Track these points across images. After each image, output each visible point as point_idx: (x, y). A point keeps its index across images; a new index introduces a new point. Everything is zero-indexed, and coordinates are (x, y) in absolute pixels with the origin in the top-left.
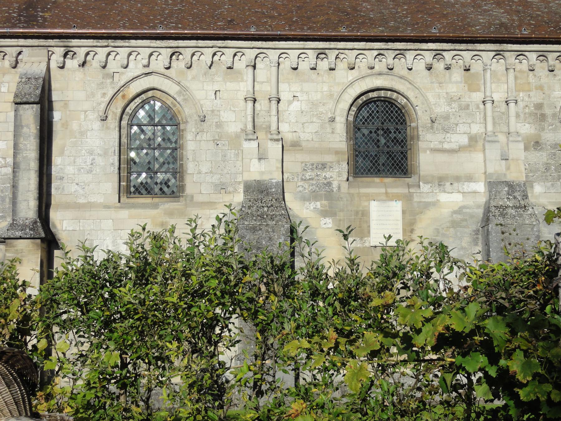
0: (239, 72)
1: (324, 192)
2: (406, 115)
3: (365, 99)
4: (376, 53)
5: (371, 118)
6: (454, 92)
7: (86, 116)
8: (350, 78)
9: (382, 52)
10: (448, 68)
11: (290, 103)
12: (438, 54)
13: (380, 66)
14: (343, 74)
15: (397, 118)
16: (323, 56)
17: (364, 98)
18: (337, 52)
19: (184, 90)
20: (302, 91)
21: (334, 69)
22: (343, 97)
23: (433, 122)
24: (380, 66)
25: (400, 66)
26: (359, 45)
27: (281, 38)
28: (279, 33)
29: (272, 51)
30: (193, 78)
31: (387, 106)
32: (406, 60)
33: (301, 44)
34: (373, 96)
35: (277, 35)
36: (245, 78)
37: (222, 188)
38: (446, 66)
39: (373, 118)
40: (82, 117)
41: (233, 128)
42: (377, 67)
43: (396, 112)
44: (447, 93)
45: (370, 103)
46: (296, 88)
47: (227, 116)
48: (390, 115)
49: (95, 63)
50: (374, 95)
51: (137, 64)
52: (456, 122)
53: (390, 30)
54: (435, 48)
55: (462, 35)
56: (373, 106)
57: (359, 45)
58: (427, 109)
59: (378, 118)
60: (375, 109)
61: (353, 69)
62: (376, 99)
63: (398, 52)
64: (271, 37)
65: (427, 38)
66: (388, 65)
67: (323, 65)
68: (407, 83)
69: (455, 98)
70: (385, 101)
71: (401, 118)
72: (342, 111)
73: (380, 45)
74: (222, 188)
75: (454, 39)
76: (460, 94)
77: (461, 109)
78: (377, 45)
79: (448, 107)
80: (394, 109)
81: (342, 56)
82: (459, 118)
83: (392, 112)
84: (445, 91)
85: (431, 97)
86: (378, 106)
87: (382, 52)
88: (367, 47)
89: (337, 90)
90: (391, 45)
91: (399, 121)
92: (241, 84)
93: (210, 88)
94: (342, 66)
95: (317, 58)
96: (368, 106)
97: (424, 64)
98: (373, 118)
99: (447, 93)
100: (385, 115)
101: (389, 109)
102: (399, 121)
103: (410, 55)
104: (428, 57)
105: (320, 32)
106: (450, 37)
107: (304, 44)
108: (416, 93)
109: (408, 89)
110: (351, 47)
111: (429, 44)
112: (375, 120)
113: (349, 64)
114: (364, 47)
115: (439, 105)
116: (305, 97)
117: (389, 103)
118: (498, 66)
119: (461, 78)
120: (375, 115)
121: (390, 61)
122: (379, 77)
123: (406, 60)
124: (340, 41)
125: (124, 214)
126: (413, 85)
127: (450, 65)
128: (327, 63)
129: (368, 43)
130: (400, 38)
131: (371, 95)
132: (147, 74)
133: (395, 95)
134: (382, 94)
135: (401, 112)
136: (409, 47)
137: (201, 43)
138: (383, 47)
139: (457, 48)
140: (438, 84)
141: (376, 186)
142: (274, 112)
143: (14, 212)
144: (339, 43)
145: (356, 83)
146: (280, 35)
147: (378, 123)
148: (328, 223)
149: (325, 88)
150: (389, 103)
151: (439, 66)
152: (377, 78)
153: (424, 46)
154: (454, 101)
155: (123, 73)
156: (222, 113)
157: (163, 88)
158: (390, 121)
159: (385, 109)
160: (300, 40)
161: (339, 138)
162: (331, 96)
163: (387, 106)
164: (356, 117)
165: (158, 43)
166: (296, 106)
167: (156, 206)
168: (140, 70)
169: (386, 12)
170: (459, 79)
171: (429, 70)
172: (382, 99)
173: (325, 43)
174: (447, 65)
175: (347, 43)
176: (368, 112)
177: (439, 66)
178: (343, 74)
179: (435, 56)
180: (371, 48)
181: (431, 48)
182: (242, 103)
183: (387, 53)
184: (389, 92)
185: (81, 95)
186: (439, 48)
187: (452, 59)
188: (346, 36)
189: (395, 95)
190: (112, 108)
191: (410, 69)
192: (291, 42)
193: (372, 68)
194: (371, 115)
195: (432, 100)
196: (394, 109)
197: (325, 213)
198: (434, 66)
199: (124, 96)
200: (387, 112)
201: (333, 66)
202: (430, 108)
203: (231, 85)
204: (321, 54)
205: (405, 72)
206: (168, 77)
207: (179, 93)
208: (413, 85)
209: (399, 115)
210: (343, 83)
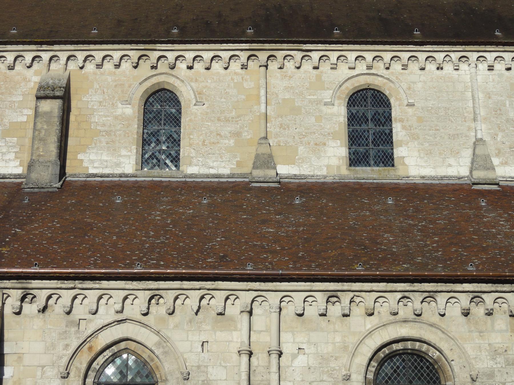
0: (232, 319)
2: (439, 371)
3: (387, 352)
4: (399, 295)
5: (395, 375)
6: (498, 343)
7: (43, 373)
8: (369, 326)
9: (406, 294)
10: (489, 314)
11: (294, 357)
12: (476, 297)
13: (405, 312)
14: (359, 322)
15: (428, 375)
16: (335, 299)
17: (386, 351)
18: (351, 294)
19: (164, 340)
20: (309, 342)
21: (349, 316)
22: (360, 350)
23: (473, 380)
24: (405, 312)
25: (430, 311)
26: (378, 286)
27: (283, 278)
28: (281, 272)
29: (272, 294)
30: (176, 326)
31: (415, 360)
32: (437, 303)
33: (308, 286)
34: (398, 348)
35: (278, 275)
36: (239, 326)
38: (487, 312)
39: (398, 375)
40: (39, 373)
42: (401, 313)
43: (428, 368)
44: (489, 344)
45: (395, 356)
46: (301, 338)
48: (419, 371)
49: (58, 308)
50: (399, 346)
52: (503, 380)
53: (416, 267)
54: (472, 289)
55: (504, 274)
56: (398, 360)
57: (378, 286)
58: (465, 364)
59: (404, 375)
60: (401, 364)
61: (372, 314)
62: (401, 352)
63: (427, 294)
64: (270, 277)
65: (462, 278)
66: (415, 310)
67: (335, 310)
68: (439, 333)
69: (500, 351)
70: (412, 354)
71: (434, 375)
73: (404, 287)
75: (495, 278)
76: (505, 345)
77: (508, 365)
78: (401, 286)
79: (491, 362)
80: (425, 364)
81: (357, 300)
82: (506, 375)
83: (422, 368)
84: (487, 342)
85: (470, 349)
86: (404, 360)
87: (406, 294)
88: (389, 289)
89: (352, 340)
90: (417, 286)
91: (431, 378)
92: (235, 334)
93: (198, 338)
94: (358, 311)
95: (327, 302)
96: (392, 361)
97: (460, 309)
98: (398, 375)
99: (489, 344)
100: (413, 371)
101: (419, 364)
102: (431, 378)
103: (442, 298)
104: (464, 300)
105: (331, 270)
106: (490, 276)
107: (310, 286)
108: (451, 344)
109: (441, 339)
110: (369, 289)
111: (465, 285)
112: (402, 378)
113: (367, 309)
114: (384, 289)
115: (480, 359)
116: (313, 350)
117: (419, 356)
119: (507, 326)
120: (401, 371)
121: (417, 305)
122: (404, 325)
123: (437, 303)
124: (355, 282)
126: (446, 334)
127: (492, 309)
128: (340, 308)
129: (389, 284)
130: (428, 278)
131: (395, 347)
132: (120, 322)
133: (425, 347)
134: (409, 345)
135: (434, 368)
136: (439, 289)
137: (186, 284)
138: (408, 288)
139: (499, 289)
140: (478, 334)
142: (274, 368)
144: (353, 284)
145: (376, 333)
146: (282, 275)
147: (404, 381)
149: (338, 339)
150: (418, 356)
151: (479, 311)
152: (401, 326)
153: (459, 287)
154: (500, 354)
155: (91, 321)
156: (210, 369)
157: (139, 339)
158: (419, 379)
159: (413, 364)
160: (305, 281)
162: (345, 348)
163: (415, 360)
164: (377, 374)
165: (135, 284)
166: (301, 361)
168: (113, 317)
169: (412, 245)
170: (504, 327)
171: (466, 316)
172: (409, 351)
173: (336, 284)
174: (488, 309)
175: (364, 284)
176: (392, 368)
177: (479, 311)
178: (359, 322)
179: (472, 299)
180: (393, 289)
181: (467, 289)
182: (235, 356)
183: (414, 296)
184: (418, 344)
185: (38, 347)
186: (477, 289)
187: (494, 303)
188: (363, 275)
189: (425, 347)
190: (76, 362)
191: (443, 315)
192: (296, 283)
193: (396, 314)
194: (395, 371)
195: (471, 353)
196: (425, 364)
198: (471, 311)
199: (90, 348)
200: (416, 368)
201: (347, 312)
202: (469, 364)
203: (221, 335)
204: (332, 297)
205: (436, 319)
206: (145, 326)
207: (158, 344)
208: (446, 334)
209: (431, 371)
210: (360, 332)
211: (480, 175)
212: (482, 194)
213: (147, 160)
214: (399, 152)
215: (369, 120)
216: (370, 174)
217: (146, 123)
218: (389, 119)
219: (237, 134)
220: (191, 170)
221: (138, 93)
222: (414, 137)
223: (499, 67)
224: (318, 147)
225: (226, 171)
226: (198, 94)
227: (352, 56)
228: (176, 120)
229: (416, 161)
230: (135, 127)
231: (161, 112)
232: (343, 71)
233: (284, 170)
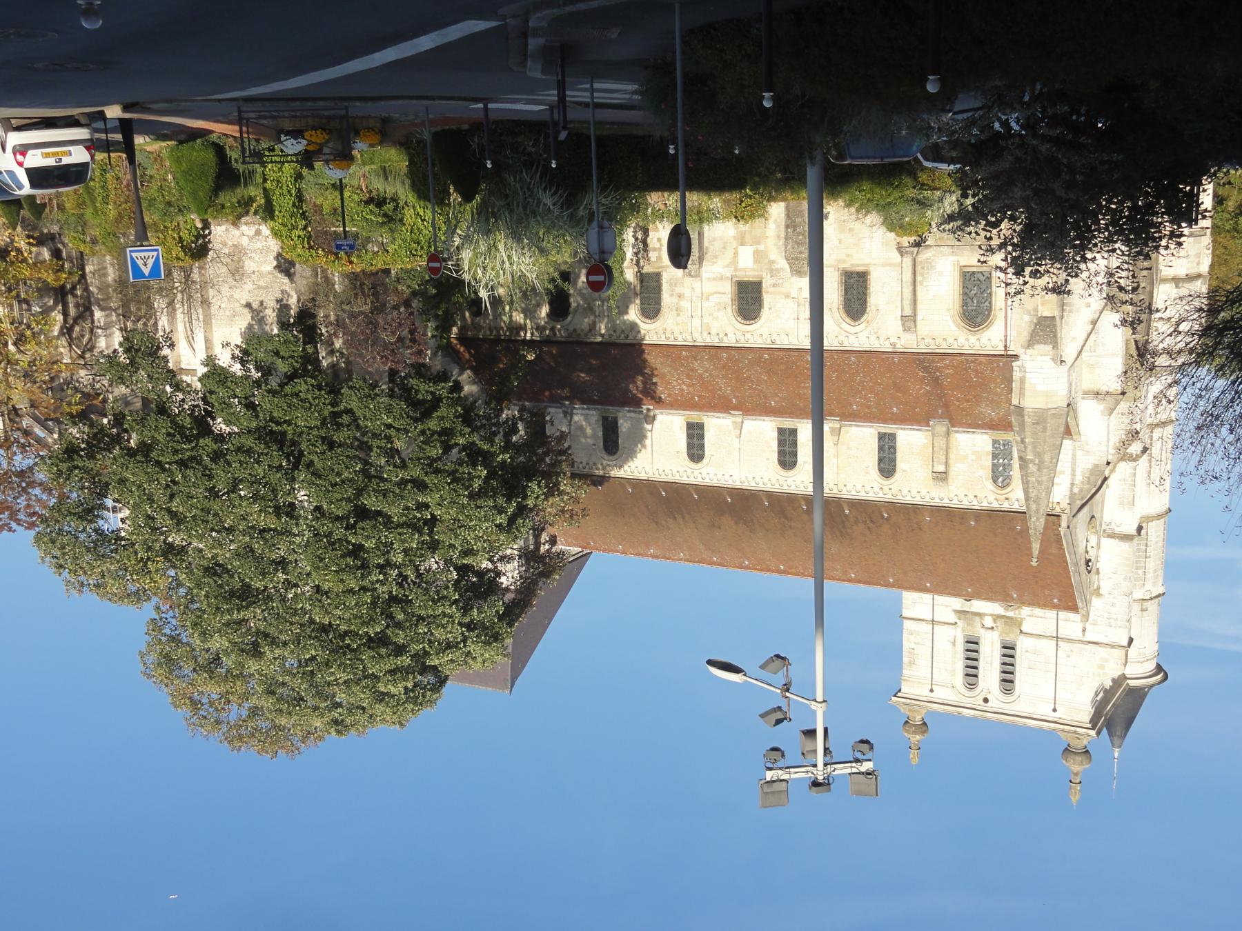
1: (773, 273)
12: (721, 341)
13: (748, 336)
72: (765, 312)
104: (725, 339)
118: (696, 335)
125: (866, 261)
141: (750, 276)
143: (914, 260)
148: (772, 258)
150: (745, 318)
161: (767, 299)
167: (852, 265)
177: (721, 335)
197: (773, 262)
213: (893, 437)
214: (776, 434)
216: (788, 423)
217: (895, 460)
218: (779, 453)
220: (872, 430)
221: (897, 475)
223: (727, 477)
225: (854, 428)
227: (793, 487)
228: (880, 460)
230: (899, 456)
231: (887, 465)
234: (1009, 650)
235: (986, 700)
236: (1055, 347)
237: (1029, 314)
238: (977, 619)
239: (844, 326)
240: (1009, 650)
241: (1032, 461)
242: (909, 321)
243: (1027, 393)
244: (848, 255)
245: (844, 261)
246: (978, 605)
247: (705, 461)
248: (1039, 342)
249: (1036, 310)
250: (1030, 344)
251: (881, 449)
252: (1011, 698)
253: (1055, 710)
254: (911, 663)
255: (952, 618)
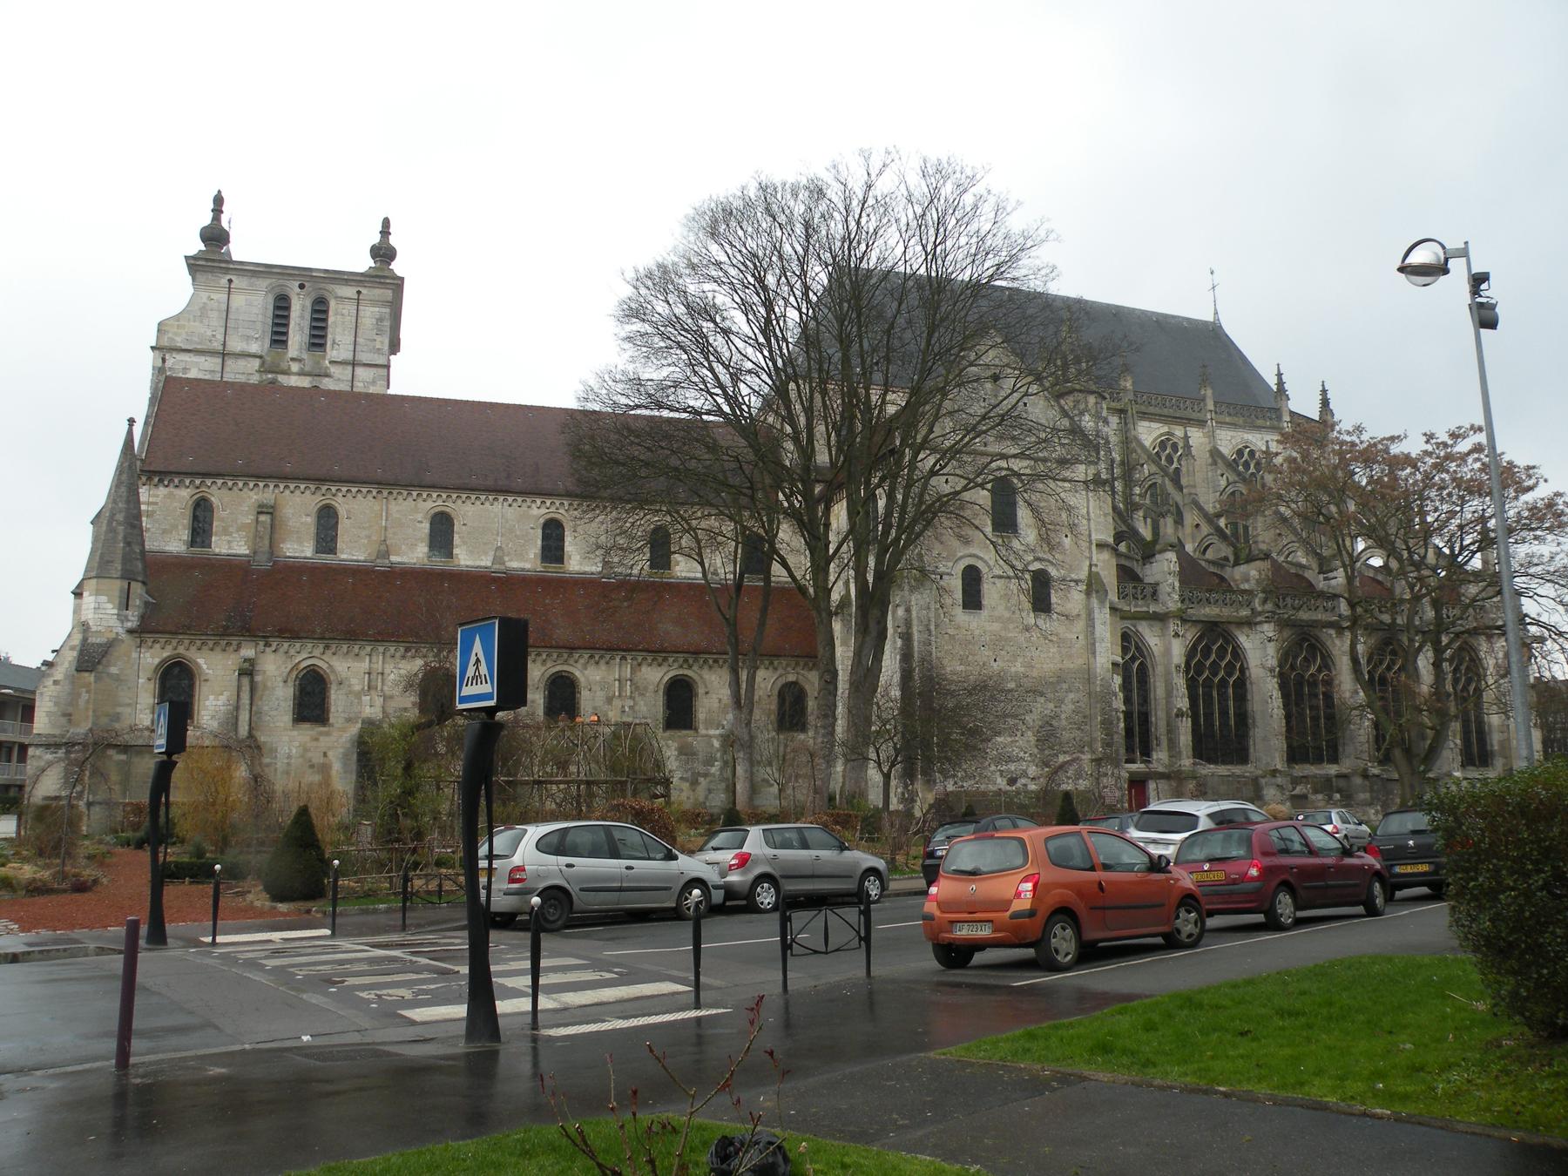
37: (349, 720)
41: (357, 688)
47: (354, 681)
51: (305, 655)
74: (349, 720)
211: (497, 567)
212: (495, 580)
214: (455, 551)
215: (442, 531)
219: (369, 537)
220: (344, 556)
222: (465, 543)
224: (413, 546)
226: (348, 511)
229: (465, 557)
230: (313, 530)
231: (327, 521)
232: (430, 504)
233: (394, 559)
234: (279, 338)
235: (302, 286)
236: (85, 640)
237: (110, 675)
238: (307, 369)
239: (325, 666)
240: (279, 338)
241: (119, 523)
242: (248, 671)
243: (117, 593)
244: (317, 740)
245: (321, 734)
246: (305, 382)
247: (542, 521)
248: (100, 645)
249: (97, 679)
250: (108, 647)
251: (334, 539)
252: (278, 291)
253: (230, 281)
254: (380, 320)
255: (333, 369)
